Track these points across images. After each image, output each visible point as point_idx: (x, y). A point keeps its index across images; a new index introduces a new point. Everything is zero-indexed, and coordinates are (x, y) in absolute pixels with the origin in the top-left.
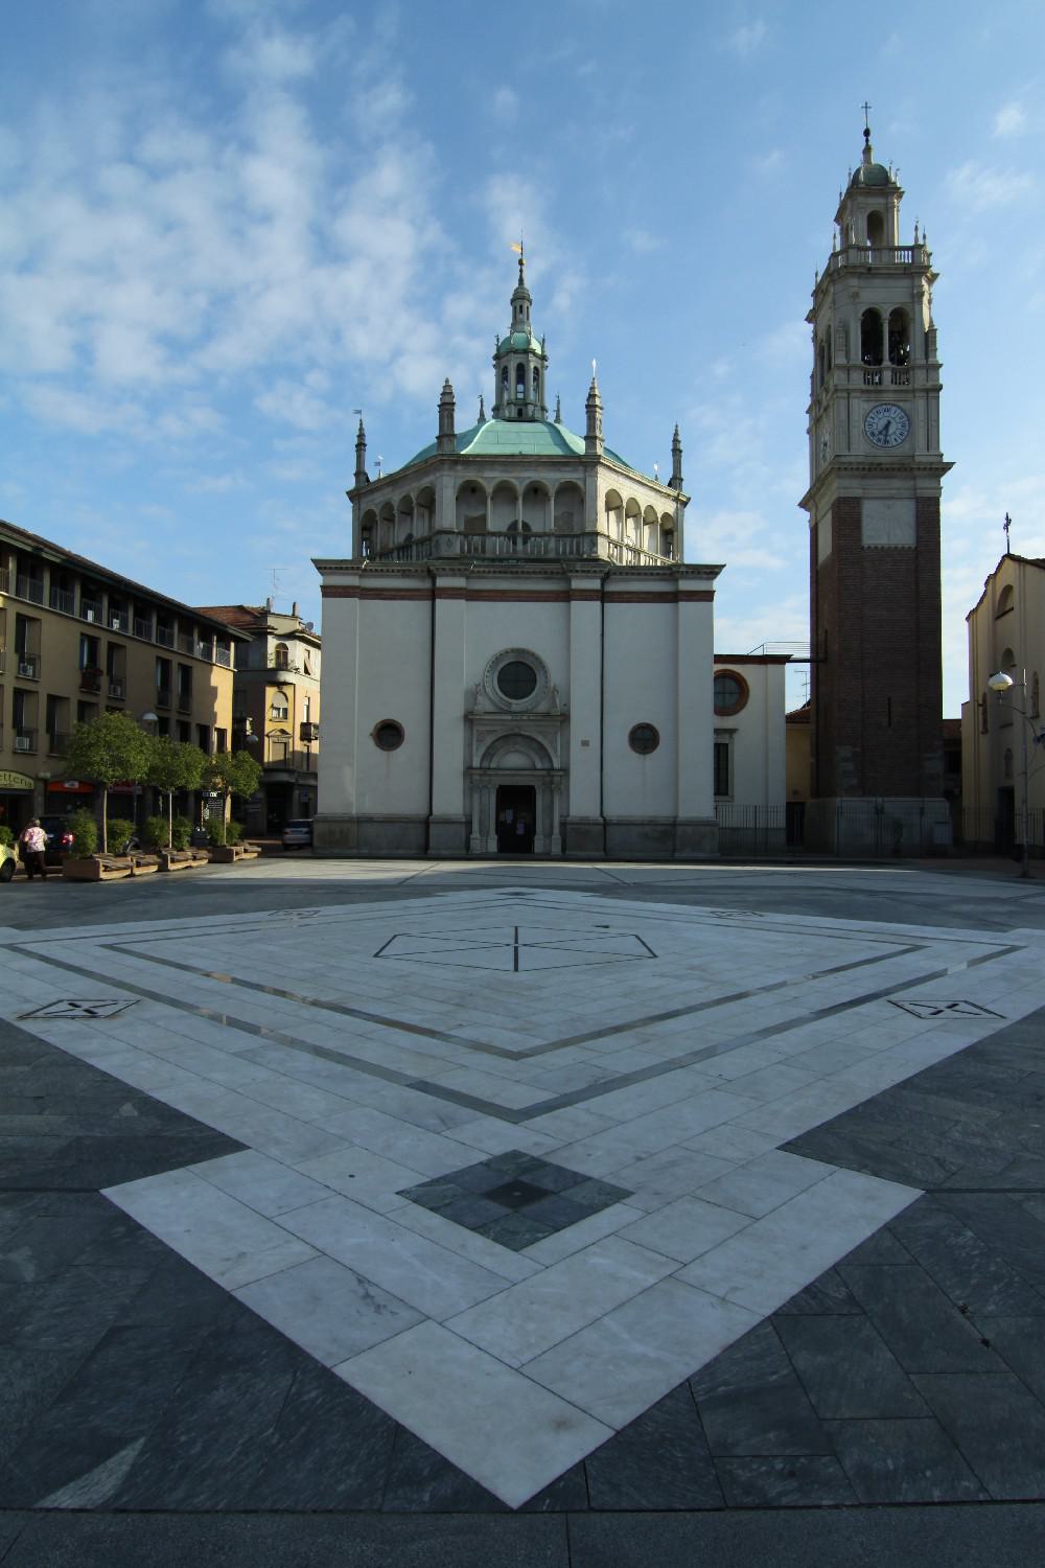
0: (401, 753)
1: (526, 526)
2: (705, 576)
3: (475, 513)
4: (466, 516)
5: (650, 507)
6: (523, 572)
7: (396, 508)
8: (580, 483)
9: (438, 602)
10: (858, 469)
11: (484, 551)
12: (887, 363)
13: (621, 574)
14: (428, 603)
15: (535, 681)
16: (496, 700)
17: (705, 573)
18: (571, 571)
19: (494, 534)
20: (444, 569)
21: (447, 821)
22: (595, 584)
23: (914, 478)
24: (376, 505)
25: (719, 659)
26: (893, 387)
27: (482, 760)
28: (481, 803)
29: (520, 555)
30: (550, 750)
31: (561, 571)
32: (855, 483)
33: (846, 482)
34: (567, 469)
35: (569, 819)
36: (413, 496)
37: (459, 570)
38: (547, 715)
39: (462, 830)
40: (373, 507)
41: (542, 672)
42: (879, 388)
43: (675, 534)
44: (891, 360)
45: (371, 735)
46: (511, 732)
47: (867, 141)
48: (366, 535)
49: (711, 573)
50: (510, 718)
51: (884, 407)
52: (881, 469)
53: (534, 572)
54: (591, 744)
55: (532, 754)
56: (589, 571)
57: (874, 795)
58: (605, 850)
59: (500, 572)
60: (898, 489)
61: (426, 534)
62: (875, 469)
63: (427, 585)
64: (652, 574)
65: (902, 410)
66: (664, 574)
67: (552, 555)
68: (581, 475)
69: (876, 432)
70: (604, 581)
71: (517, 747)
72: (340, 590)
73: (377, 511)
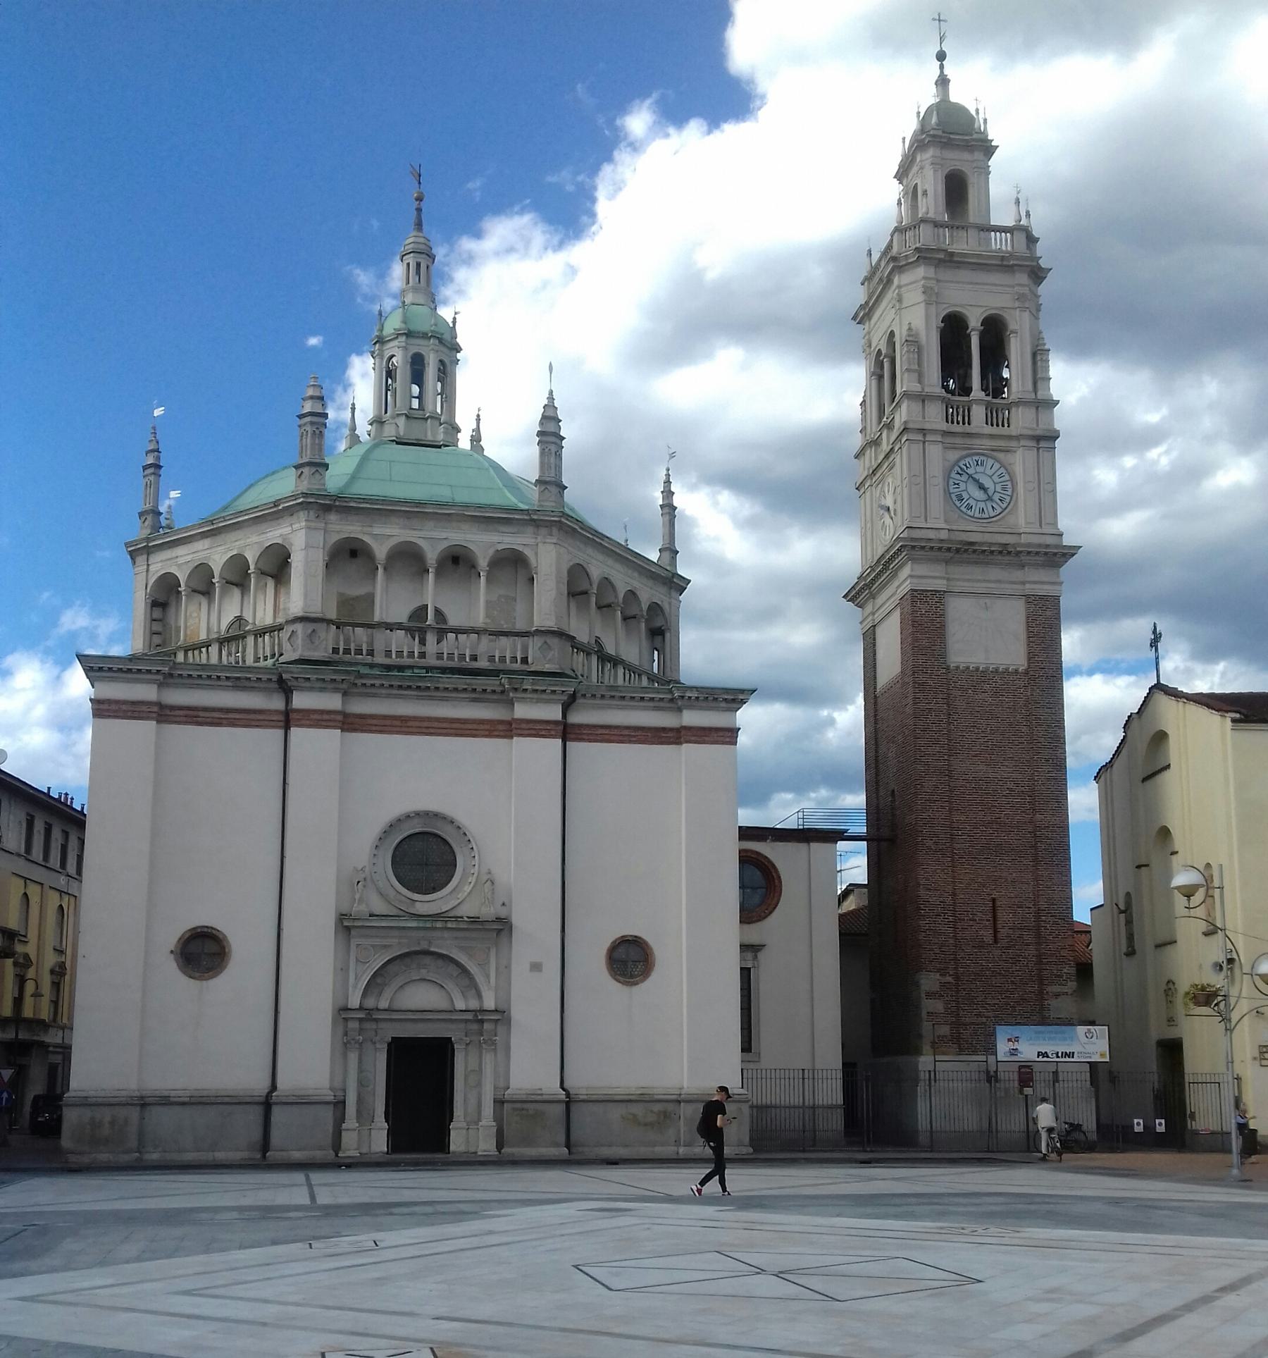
0: (221, 985)
1: (438, 613)
2: (723, 704)
3: (358, 590)
4: (341, 595)
5: (632, 594)
6: (437, 688)
7: (217, 574)
10: (940, 549)
11: (371, 653)
12: (977, 392)
13: (594, 696)
14: (283, 731)
15: (456, 866)
16: (392, 894)
18: (516, 689)
19: (390, 627)
21: (302, 1102)
23: (1023, 566)
24: (179, 566)
25: (747, 833)
26: (988, 430)
27: (365, 994)
28: (361, 1070)
29: (432, 661)
30: (479, 979)
31: (499, 689)
32: (938, 570)
33: (922, 569)
34: (510, 529)
35: (509, 1091)
38: (474, 920)
39: (328, 1114)
42: (967, 428)
43: (668, 635)
44: (984, 388)
45: (172, 952)
46: (418, 949)
48: (157, 613)
49: (734, 700)
50: (414, 924)
52: (975, 551)
53: (456, 690)
55: (450, 985)
58: (568, 1146)
59: (400, 687)
60: (999, 581)
61: (269, 621)
62: (966, 551)
63: (277, 703)
64: (642, 698)
65: (1002, 466)
66: (661, 699)
67: (483, 664)
68: (531, 541)
69: (965, 496)
71: (424, 971)
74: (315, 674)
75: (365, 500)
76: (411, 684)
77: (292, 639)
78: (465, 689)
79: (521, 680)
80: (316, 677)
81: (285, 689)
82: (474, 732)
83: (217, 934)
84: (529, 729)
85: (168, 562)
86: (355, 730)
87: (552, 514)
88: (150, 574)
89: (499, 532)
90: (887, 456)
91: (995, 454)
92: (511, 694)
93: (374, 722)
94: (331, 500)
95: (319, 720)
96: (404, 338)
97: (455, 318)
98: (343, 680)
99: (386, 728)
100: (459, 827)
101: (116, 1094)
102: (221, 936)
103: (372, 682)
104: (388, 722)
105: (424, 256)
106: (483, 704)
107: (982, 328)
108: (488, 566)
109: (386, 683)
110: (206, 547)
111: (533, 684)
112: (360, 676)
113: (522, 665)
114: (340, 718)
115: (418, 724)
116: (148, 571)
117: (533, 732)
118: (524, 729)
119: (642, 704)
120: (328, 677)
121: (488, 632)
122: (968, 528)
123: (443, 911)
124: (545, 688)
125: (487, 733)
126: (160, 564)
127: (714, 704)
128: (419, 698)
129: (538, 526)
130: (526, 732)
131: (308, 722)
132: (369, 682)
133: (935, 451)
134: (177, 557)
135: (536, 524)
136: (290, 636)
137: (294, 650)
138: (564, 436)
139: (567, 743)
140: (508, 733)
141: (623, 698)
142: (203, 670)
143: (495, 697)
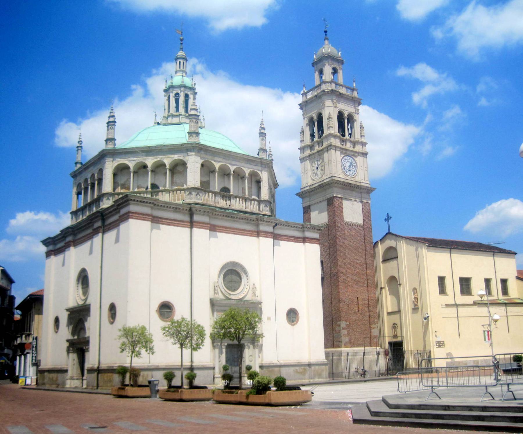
2: (316, 231)
3: (205, 179)
8: (259, 172)
14: (190, 229)
16: (223, 291)
17: (317, 229)
18: (261, 220)
20: (200, 211)
22: (270, 229)
23: (361, 193)
41: (245, 276)
47: (326, 35)
49: (319, 230)
51: (348, 157)
53: (242, 219)
54: (271, 319)
56: (269, 222)
57: (354, 347)
59: (226, 216)
66: (299, 227)
69: (345, 167)
70: (274, 227)
78: (245, 219)
83: (171, 305)
89: (251, 164)
90: (318, 152)
91: (352, 157)
92: (260, 222)
99: (222, 231)
100: (243, 268)
101: (142, 365)
102: (171, 305)
107: (348, 117)
109: (222, 214)
112: (216, 211)
114: (209, 226)
117: (266, 236)
119: (294, 228)
120: (207, 211)
122: (347, 179)
123: (240, 298)
124: (269, 220)
125: (250, 235)
127: (314, 231)
130: (264, 235)
131: (199, 227)
132: (217, 213)
133: (338, 153)
141: (289, 226)
143: (253, 222)
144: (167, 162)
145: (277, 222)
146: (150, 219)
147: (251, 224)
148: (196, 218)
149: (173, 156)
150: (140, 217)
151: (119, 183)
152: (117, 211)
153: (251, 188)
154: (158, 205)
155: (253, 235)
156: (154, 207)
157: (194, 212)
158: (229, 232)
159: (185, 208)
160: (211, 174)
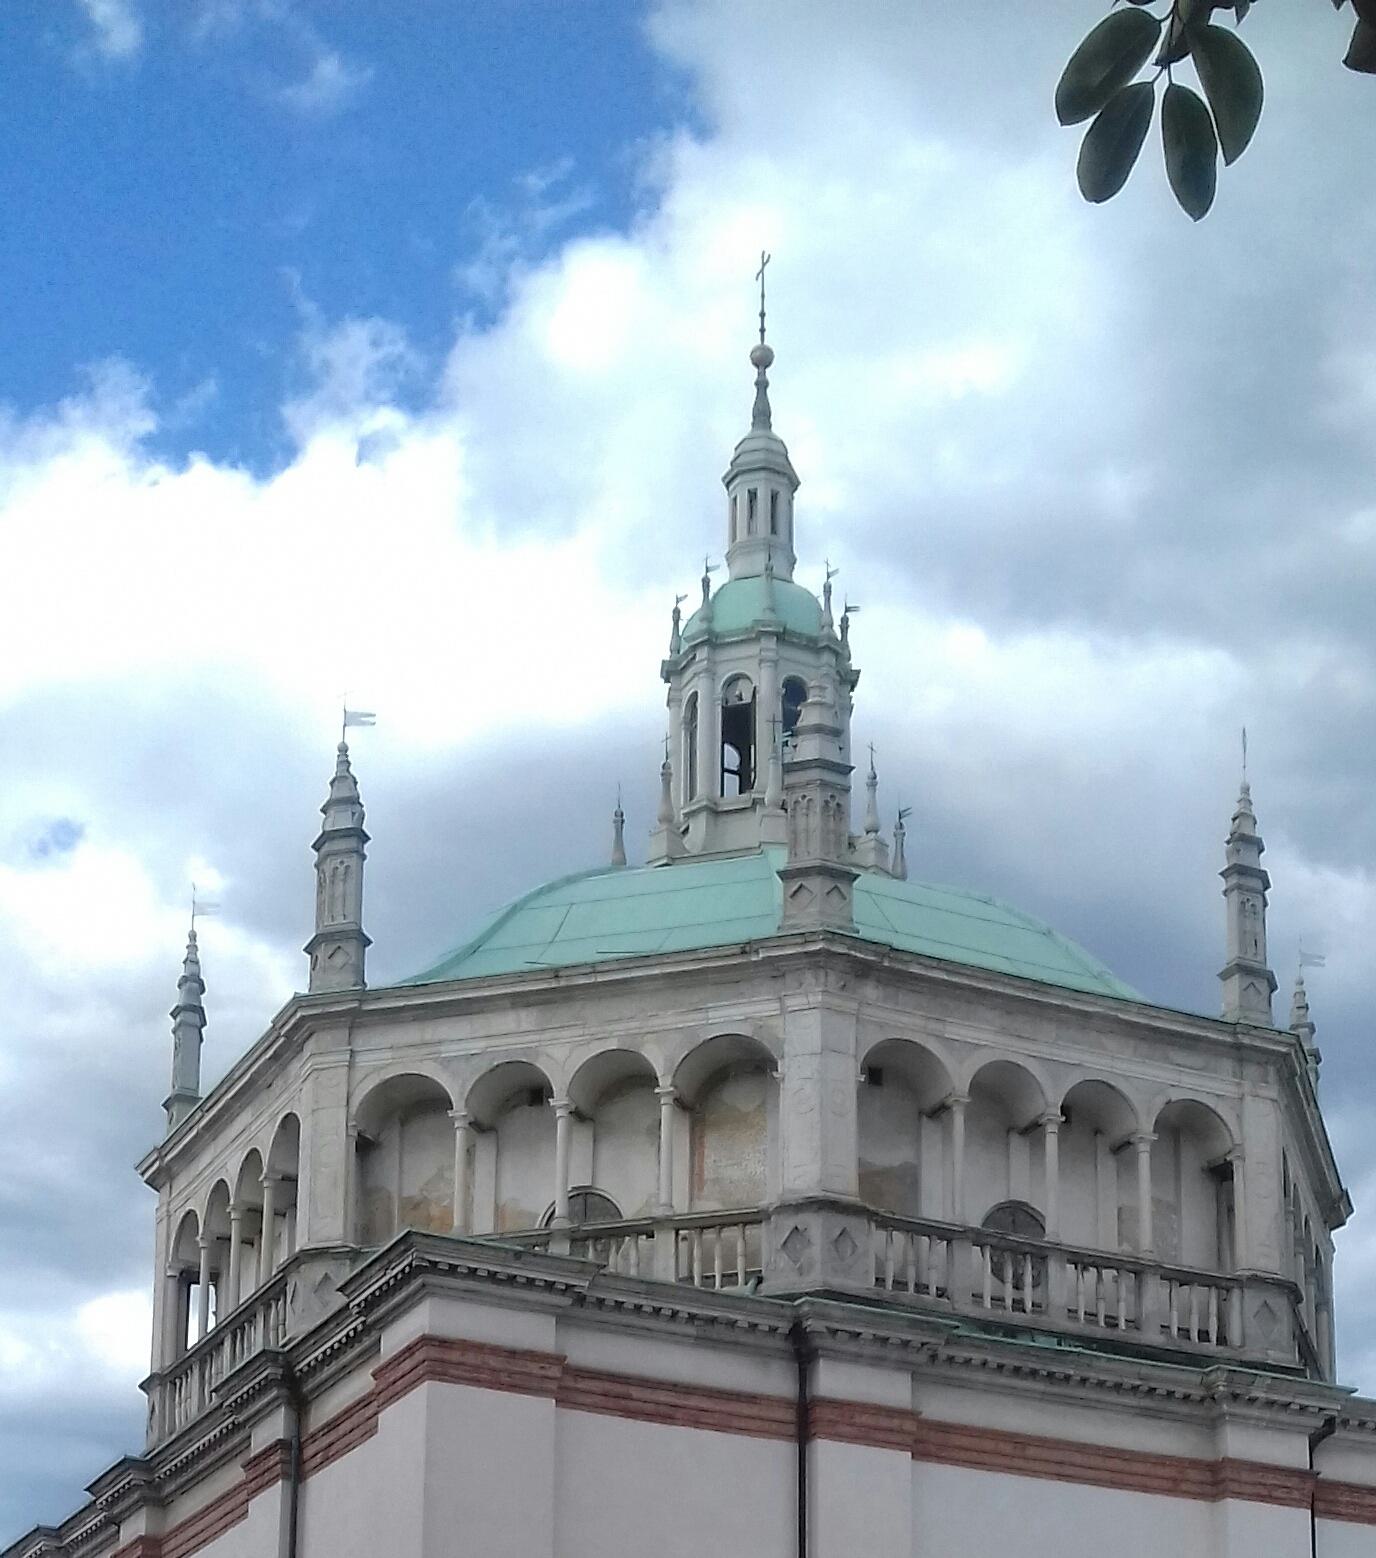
6: (1084, 1381)
9: (825, 1450)
13: (1362, 1424)
18: (1235, 1397)
22: (1291, 1451)
24: (446, 1063)
31: (1197, 1393)
36: (661, 1059)
37: (906, 1344)
40: (428, 1070)
53: (1118, 1387)
56: (1287, 1405)
59: (1017, 1371)
63: (776, 1381)
67: (1152, 1337)
68: (1228, 1089)
72: (494, 1362)
73: (456, 1089)
74: (868, 1324)
75: (940, 962)
76: (1037, 1366)
77: (789, 1245)
78: (1135, 1389)
79: (1251, 1379)
80: (872, 1331)
81: (802, 1351)
82: (1148, 1482)
84: (1254, 1484)
85: (412, 1051)
86: (940, 1459)
87: (1279, 1038)
88: (358, 1075)
92: (1225, 1407)
93: (965, 1441)
94: (876, 954)
95: (870, 1427)
96: (772, 643)
97: (845, 621)
98: (923, 1344)
99: (986, 1458)
103: (966, 1355)
104: (988, 1445)
105: (785, 481)
106: (1163, 1423)
108: (1155, 1132)
109: (993, 1360)
110: (525, 1027)
111: (1270, 1389)
113: (1221, 1348)
114: (909, 1426)
115: (1046, 1454)
116: (351, 1066)
118: (1246, 1483)
120: (896, 1335)
121: (1161, 1271)
124: (1289, 1400)
126: (389, 1054)
128: (1044, 1398)
129: (1241, 1061)
130: (1248, 1489)
131: (847, 1429)
132: (961, 1354)
134: (440, 1042)
135: (1240, 1053)
136: (788, 1237)
137: (801, 1271)
138: (1220, 876)
139: (1316, 1520)
140: (1208, 1489)
142: (648, 1294)
143: (1184, 1409)
144: (661, 1061)
145: (1334, 1408)
146: (553, 1386)
147: (1174, 1418)
148: (833, 1380)
149: (692, 1020)
150: (494, 1370)
151: (393, 1188)
152: (367, 1342)
153: (1176, 1209)
154: (601, 1302)
155: (1184, 1487)
156: (579, 1312)
157: (818, 1342)
158: (1037, 1466)
159: (764, 1323)
160: (929, 1127)
